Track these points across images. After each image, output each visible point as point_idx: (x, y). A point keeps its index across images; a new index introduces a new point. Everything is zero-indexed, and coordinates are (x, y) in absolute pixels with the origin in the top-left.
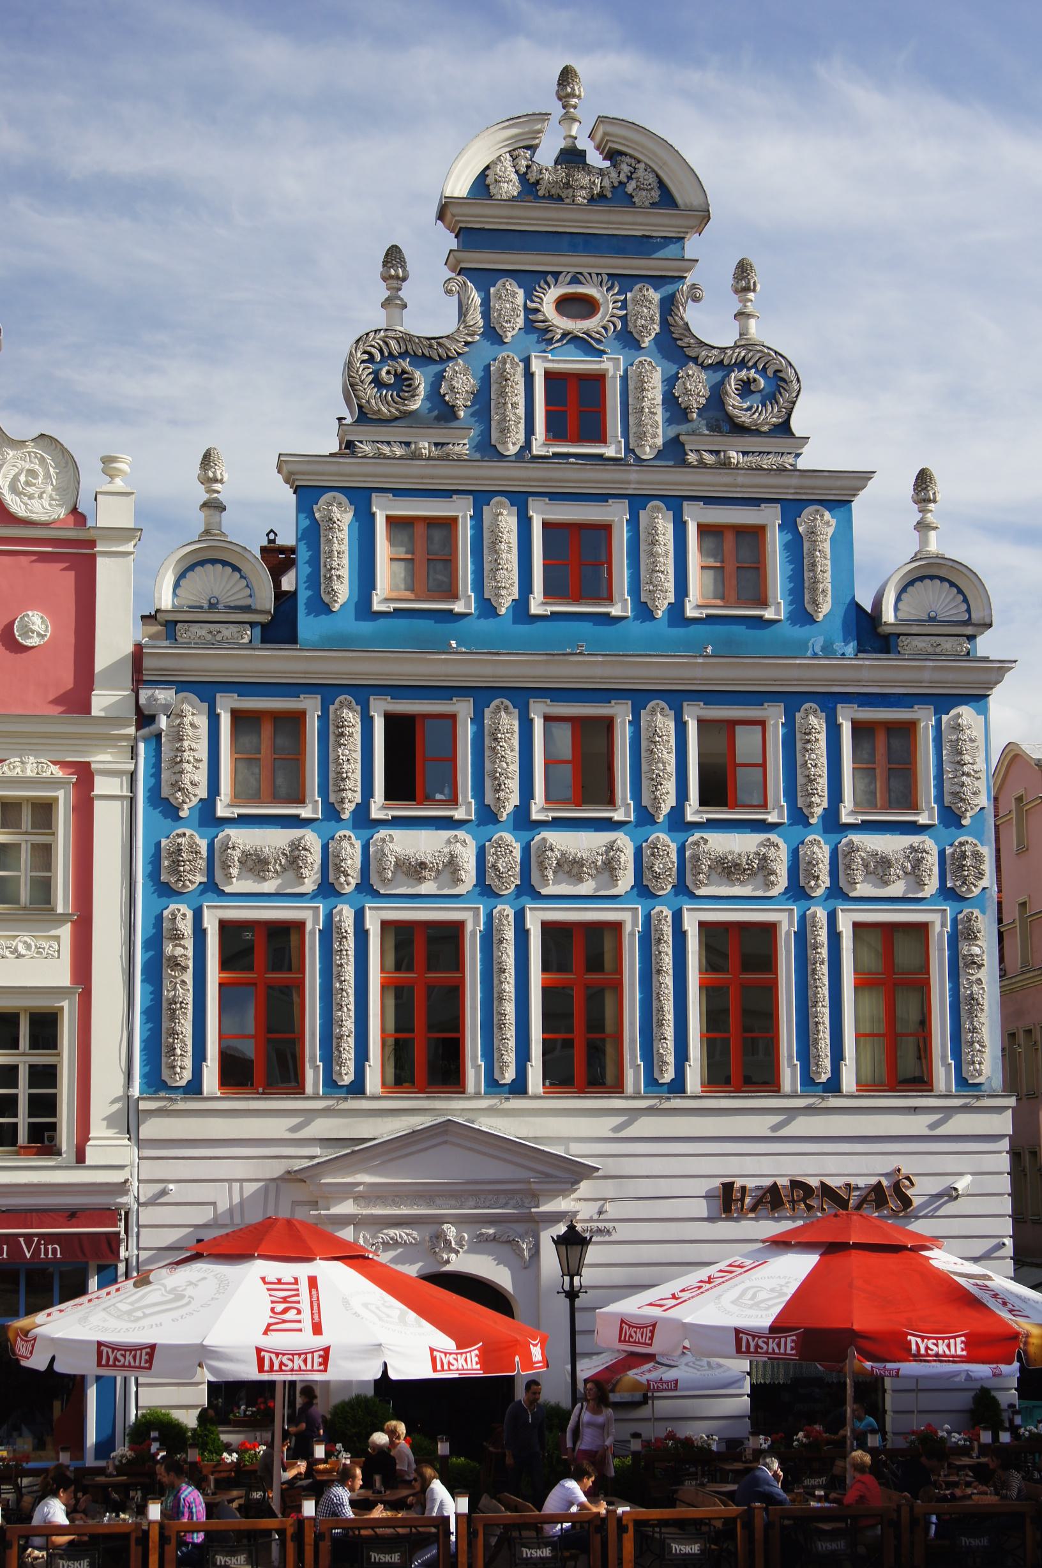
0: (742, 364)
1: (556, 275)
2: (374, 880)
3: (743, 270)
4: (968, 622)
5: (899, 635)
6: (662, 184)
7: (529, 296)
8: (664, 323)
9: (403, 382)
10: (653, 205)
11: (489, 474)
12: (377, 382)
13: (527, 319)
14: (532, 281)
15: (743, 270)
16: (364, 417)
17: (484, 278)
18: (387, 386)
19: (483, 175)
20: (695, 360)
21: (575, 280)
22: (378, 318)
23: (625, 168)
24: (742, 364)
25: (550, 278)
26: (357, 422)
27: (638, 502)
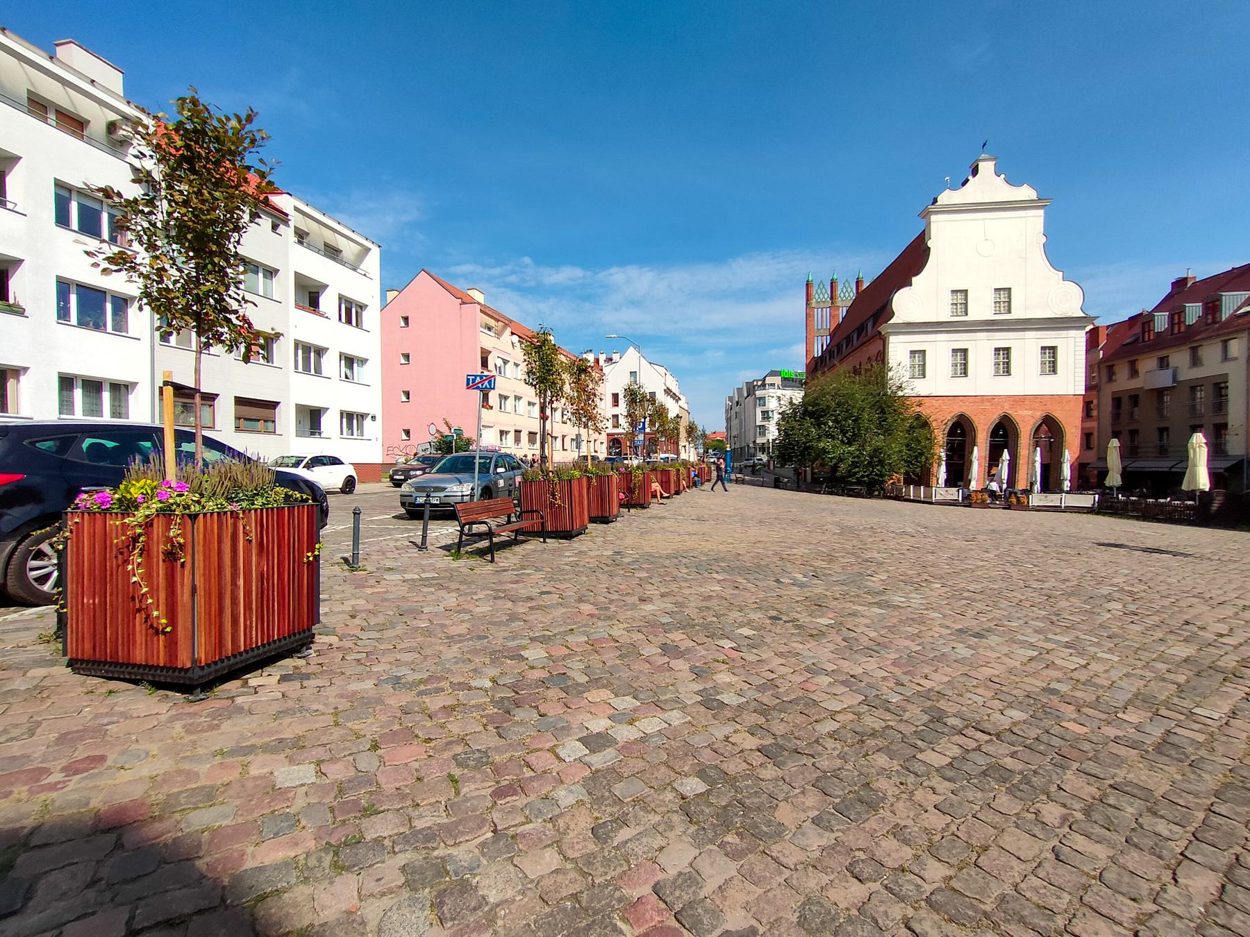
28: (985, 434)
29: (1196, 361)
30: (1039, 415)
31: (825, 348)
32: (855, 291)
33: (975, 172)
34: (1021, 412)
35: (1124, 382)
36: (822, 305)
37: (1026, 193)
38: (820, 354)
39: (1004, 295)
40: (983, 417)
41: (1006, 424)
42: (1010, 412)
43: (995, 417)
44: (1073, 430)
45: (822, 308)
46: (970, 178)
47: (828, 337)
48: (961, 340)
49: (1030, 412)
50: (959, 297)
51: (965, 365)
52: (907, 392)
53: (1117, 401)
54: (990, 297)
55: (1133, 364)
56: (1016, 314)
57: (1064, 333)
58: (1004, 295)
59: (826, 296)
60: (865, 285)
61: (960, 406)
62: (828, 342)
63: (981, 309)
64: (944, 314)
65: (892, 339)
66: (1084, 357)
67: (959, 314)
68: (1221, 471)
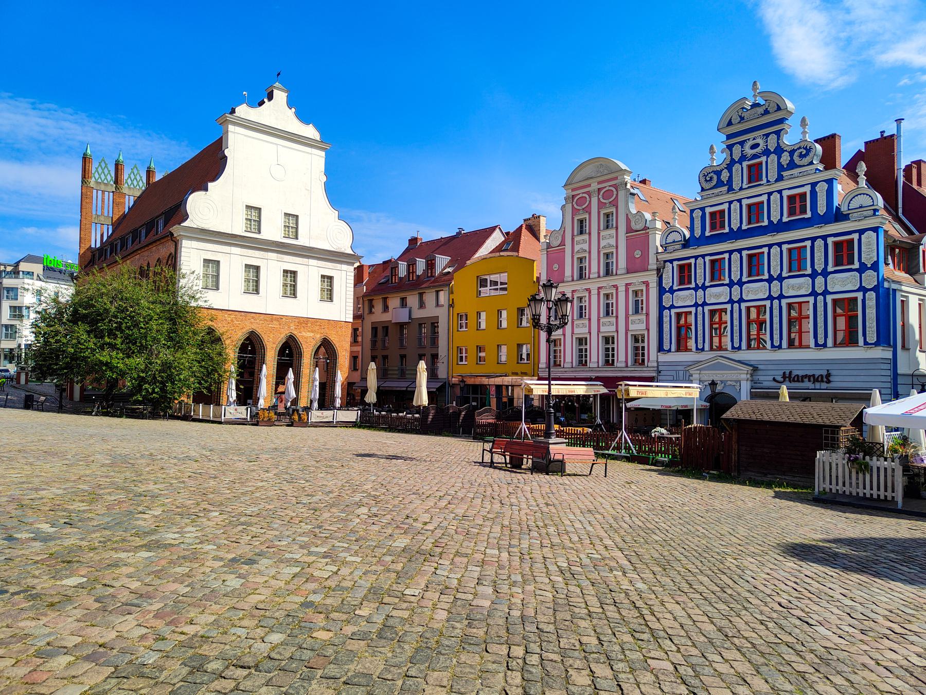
0: (800, 148)
1: (749, 139)
2: (706, 300)
3: (803, 120)
4: (873, 205)
5: (849, 214)
6: (778, 105)
7: (742, 147)
8: (778, 143)
9: (711, 178)
10: (775, 111)
11: (731, 197)
12: (706, 180)
13: (742, 154)
14: (742, 143)
15: (803, 120)
16: (703, 189)
17: (730, 147)
18: (709, 181)
19: (731, 119)
20: (786, 151)
21: (754, 139)
22: (707, 163)
23: (767, 104)
24: (800, 148)
25: (747, 141)
26: (702, 191)
27: (770, 194)
28: (273, 352)
29: (422, 305)
30: (319, 337)
31: (105, 238)
32: (145, 181)
33: (270, 97)
34: (304, 334)
35: (379, 316)
36: (103, 187)
37: (310, 132)
38: (98, 245)
39: (292, 220)
40: (272, 336)
41: (292, 344)
42: (295, 332)
43: (282, 336)
44: (344, 353)
45: (103, 192)
46: (266, 100)
47: (110, 227)
48: (291, 262)
49: (312, 334)
50: (254, 214)
51: (257, 282)
52: (201, 303)
53: (375, 330)
54: (280, 221)
55: (385, 300)
56: (303, 241)
57: (338, 266)
58: (292, 220)
59: (109, 178)
60: (158, 177)
61: (251, 323)
62: (110, 232)
63: (272, 230)
64: (239, 228)
65: (185, 243)
66: (352, 289)
67: (253, 230)
68: (435, 390)
